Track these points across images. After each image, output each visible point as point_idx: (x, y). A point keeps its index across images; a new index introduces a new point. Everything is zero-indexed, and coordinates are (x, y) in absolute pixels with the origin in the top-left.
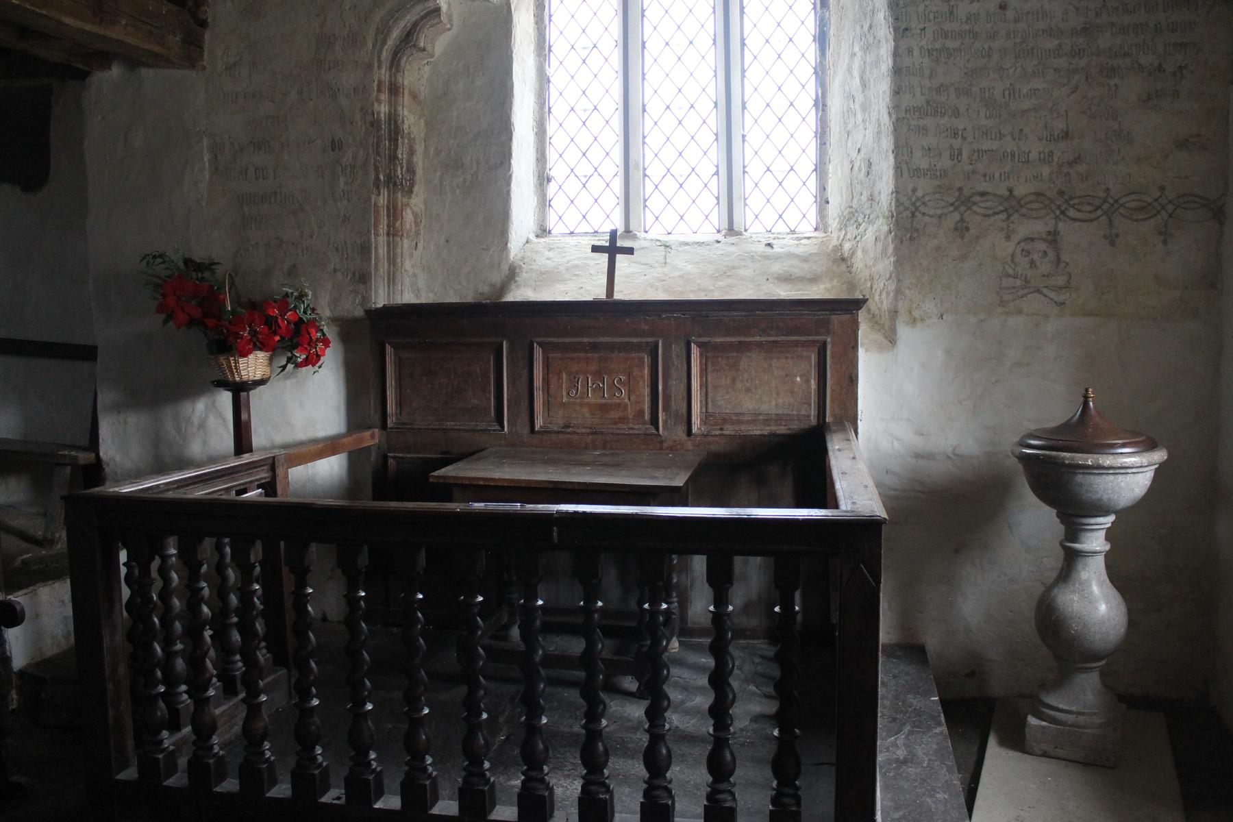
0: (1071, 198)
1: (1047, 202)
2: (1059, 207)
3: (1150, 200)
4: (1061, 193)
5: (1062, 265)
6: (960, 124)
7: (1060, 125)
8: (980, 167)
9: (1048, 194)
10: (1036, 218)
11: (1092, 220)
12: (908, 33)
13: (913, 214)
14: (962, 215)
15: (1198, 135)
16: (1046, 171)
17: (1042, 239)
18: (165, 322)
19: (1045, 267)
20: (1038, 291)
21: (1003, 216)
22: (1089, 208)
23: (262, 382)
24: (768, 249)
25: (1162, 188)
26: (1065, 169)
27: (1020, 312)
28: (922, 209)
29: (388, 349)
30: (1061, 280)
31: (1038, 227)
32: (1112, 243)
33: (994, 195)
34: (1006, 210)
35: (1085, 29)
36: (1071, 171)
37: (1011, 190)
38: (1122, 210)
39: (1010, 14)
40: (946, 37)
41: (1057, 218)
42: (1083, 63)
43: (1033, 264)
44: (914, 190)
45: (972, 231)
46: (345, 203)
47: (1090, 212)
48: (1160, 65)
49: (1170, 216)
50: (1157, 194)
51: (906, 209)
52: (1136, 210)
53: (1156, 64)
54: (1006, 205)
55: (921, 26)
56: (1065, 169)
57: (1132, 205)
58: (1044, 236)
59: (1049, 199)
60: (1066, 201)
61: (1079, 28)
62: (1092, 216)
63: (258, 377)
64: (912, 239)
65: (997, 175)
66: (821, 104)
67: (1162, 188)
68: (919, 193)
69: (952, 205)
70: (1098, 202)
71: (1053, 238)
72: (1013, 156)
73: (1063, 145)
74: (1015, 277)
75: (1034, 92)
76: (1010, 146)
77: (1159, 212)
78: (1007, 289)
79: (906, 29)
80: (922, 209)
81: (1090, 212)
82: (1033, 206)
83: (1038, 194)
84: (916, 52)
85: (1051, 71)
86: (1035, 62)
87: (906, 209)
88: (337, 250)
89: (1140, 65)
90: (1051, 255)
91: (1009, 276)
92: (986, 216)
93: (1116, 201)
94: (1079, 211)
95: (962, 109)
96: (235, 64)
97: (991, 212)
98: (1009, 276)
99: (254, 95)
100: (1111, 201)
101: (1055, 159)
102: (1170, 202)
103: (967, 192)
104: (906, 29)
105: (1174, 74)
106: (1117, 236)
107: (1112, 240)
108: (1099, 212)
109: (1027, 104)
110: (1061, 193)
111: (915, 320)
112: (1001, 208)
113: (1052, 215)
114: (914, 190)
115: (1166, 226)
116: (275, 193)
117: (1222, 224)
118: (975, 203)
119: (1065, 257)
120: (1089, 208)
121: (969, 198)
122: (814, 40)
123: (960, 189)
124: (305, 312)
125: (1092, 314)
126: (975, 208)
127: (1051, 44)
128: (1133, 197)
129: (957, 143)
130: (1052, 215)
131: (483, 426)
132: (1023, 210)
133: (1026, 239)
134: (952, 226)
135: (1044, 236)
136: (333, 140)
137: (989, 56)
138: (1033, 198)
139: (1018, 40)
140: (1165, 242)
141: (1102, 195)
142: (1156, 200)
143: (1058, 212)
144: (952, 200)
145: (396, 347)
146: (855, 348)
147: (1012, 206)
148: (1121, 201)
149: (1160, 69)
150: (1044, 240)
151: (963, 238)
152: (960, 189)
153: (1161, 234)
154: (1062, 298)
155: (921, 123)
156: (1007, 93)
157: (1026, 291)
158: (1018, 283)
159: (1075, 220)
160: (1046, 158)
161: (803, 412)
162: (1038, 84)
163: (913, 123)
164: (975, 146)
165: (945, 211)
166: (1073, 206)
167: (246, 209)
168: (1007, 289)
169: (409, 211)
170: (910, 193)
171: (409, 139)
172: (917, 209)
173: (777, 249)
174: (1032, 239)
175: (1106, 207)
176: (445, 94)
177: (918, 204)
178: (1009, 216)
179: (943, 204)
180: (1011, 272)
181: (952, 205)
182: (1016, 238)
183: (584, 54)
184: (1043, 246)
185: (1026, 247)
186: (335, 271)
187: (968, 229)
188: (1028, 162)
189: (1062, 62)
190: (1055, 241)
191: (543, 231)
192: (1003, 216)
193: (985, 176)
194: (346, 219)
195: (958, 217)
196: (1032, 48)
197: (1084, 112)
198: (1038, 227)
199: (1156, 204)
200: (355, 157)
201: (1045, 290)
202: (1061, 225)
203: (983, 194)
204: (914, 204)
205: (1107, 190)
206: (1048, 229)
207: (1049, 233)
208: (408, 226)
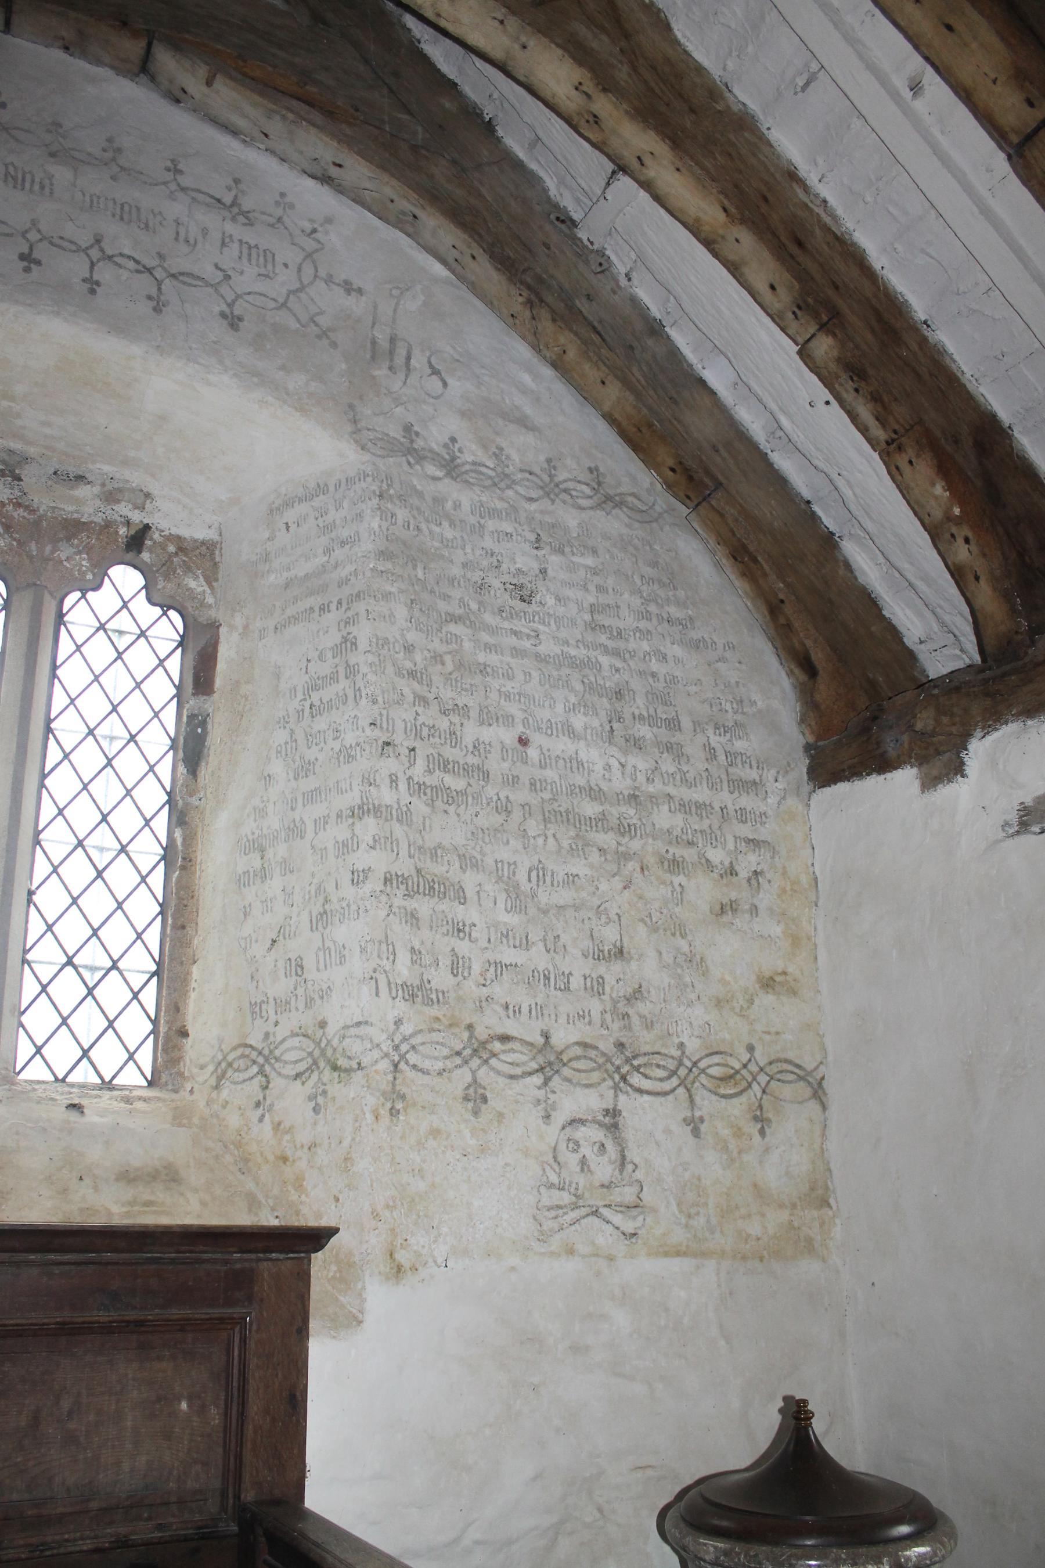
0: (635, 1057)
1: (601, 1060)
2: (618, 1068)
3: (737, 1066)
4: (620, 1046)
5: (630, 1167)
6: (468, 914)
7: (610, 935)
8: (498, 991)
9: (602, 1046)
10: (588, 1086)
11: (665, 1094)
12: (390, 748)
13: (396, 1066)
14: (474, 1073)
15: (784, 973)
16: (595, 1006)
17: (595, 1121)
19: (603, 1169)
20: (595, 1213)
21: (537, 1080)
22: (661, 1073)
24: (73, 1116)
25: (751, 1048)
26: (622, 1007)
27: (571, 1251)
28: (412, 1058)
30: (628, 1194)
31: (590, 1101)
32: (696, 1133)
33: (522, 1041)
34: (541, 1069)
35: (634, 797)
36: (631, 1011)
37: (546, 1036)
38: (703, 1079)
39: (532, 752)
40: (445, 769)
41: (616, 1087)
42: (636, 845)
43: (583, 1162)
44: (398, 1023)
45: (495, 1103)
47: (661, 1080)
48: (731, 863)
49: (764, 1092)
50: (745, 1057)
51: (387, 1055)
52: (721, 1079)
53: (727, 863)
54: (541, 1060)
55: (411, 744)
56: (622, 1007)
57: (715, 1071)
58: (601, 1118)
59: (604, 1054)
60: (628, 1061)
61: (626, 793)
62: (667, 1086)
64: (393, 1112)
65: (525, 1009)
66: (178, 859)
67: (751, 1048)
68: (407, 1029)
69: (458, 1053)
70: (671, 1065)
71: (612, 1121)
72: (547, 978)
73: (617, 967)
74: (561, 1189)
75: (571, 879)
76: (538, 958)
77: (750, 1085)
78: (550, 1209)
79: (388, 744)
80: (412, 1058)
81: (661, 1080)
82: (581, 1065)
83: (585, 1045)
84: (403, 786)
85: (595, 849)
86: (572, 833)
87: (387, 1055)
89: (707, 860)
91: (552, 1186)
92: (512, 1077)
93: (695, 1064)
94: (646, 1076)
95: (470, 892)
97: (518, 1071)
98: (552, 1186)
100: (689, 1064)
101: (607, 988)
102: (762, 1069)
103: (481, 1033)
104: (388, 744)
105: (749, 880)
106: (702, 1120)
107: (694, 1125)
108: (675, 1081)
109: (564, 896)
110: (620, 1046)
111: (399, 1268)
112: (534, 1066)
113: (610, 1083)
114: (398, 1023)
115: (760, 1107)
117: (824, 1108)
118: (494, 1055)
119: (633, 1154)
120: (661, 1073)
121: (484, 1044)
122: (173, 747)
123: (470, 1027)
125: (678, 1253)
126: (493, 1061)
127: (590, 809)
128: (716, 1059)
129: (463, 947)
130: (610, 1083)
132: (566, 1071)
134: (460, 1092)
135: (601, 1118)
137: (509, 813)
138: (578, 1051)
139: (547, 795)
140: (762, 1132)
141: (677, 1053)
142: (745, 1066)
143: (617, 1077)
144: (459, 1047)
146: (302, 1332)
147: (549, 1062)
148: (702, 1064)
149: (732, 872)
150: (601, 1124)
151: (476, 1113)
152: (470, 1027)
153: (756, 1119)
154: (629, 1227)
155: (412, 904)
156: (534, 874)
157: (574, 1215)
158: (566, 1198)
159: (640, 1091)
160: (597, 987)
161: (190, 1484)
162: (578, 867)
163: (398, 902)
164: (489, 955)
165: (448, 1063)
166: (637, 1069)
168: (550, 1209)
170: (392, 1027)
172: (402, 1057)
173: (91, 1117)
174: (582, 1122)
175: (683, 1072)
177: (404, 1047)
178: (547, 1081)
179: (446, 1052)
180: (554, 1179)
181: (458, 1053)
182: (560, 1118)
184: (597, 1134)
187: (485, 1099)
188: (567, 989)
189: (607, 839)
190: (615, 1126)
192: (537, 1080)
193: (507, 1008)
195: (468, 1078)
196: (567, 812)
197: (642, 920)
198: (590, 1101)
199: (744, 1072)
201: (605, 1212)
202: (622, 1098)
203: (505, 1038)
204: (396, 1048)
205: (681, 1045)
206: (605, 1106)
207: (607, 1112)
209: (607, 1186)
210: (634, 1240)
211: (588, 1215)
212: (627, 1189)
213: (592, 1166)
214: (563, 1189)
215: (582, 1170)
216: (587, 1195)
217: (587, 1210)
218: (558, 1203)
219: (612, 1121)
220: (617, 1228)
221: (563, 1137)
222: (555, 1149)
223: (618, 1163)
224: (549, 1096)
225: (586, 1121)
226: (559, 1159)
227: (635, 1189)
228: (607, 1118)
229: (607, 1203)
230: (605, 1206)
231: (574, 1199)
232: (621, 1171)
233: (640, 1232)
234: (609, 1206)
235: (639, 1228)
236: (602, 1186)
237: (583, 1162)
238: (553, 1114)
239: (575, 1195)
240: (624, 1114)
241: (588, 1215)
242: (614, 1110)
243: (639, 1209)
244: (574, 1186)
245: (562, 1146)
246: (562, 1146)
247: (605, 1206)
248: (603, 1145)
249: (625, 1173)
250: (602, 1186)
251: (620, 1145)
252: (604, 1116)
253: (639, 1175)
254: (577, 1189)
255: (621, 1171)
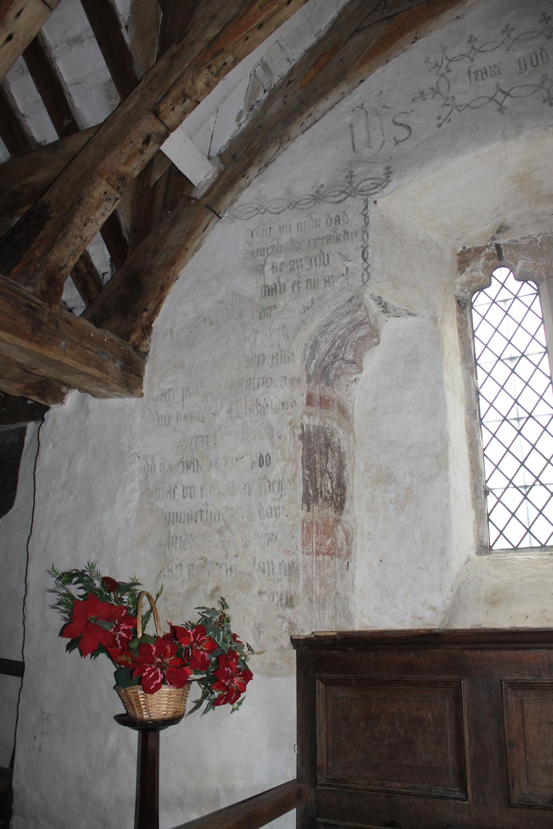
18: (70, 647)
23: (174, 720)
29: (320, 686)
46: (273, 519)
63: (170, 715)
88: (264, 571)
96: (169, 390)
99: (186, 418)
116: (201, 511)
124: (225, 641)
131: (440, 791)
136: (261, 456)
145: (329, 683)
167: (172, 528)
169: (340, 527)
171: (339, 452)
176: (374, 409)
183: (512, 365)
186: (260, 593)
191: (485, 548)
194: (272, 538)
200: (284, 473)
208: (339, 545)
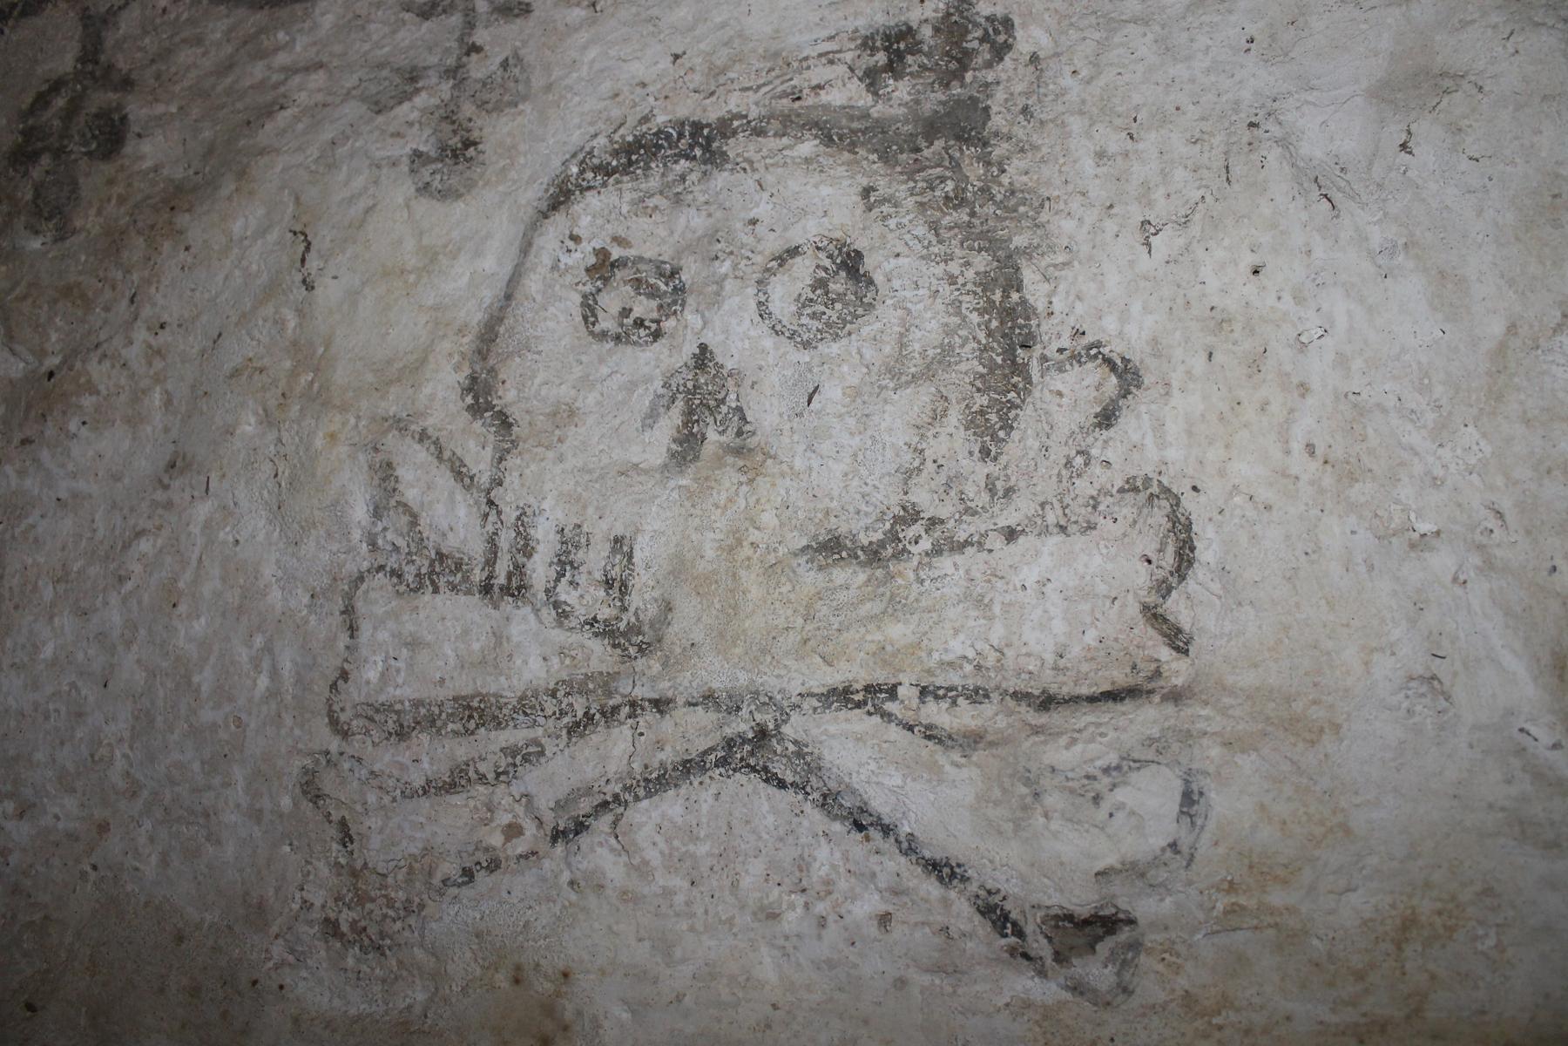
5: (1065, 395)
17: (791, 123)
20: (753, 751)
58: (845, 93)
90: (920, 289)
91: (441, 570)
98: (441, 570)
133: (636, 153)
135: (844, 93)
150: (838, 134)
174: (704, 142)
180: (455, 521)
184: (818, 198)
185: (652, 238)
190: (963, 125)
207: (893, 49)
209: (869, 554)
210: (1097, 971)
211: (689, 767)
212: (1038, 560)
213: (768, 411)
214: (516, 589)
215: (688, 445)
216: (690, 620)
217: (695, 729)
218: (463, 684)
219: (934, 100)
220: (944, 871)
221: (561, 254)
222: (488, 336)
223: (969, 364)
224: (481, 36)
225: (725, 128)
226: (507, 396)
227: (1117, 562)
228: (901, 90)
229: (856, 672)
230: (841, 696)
231: (599, 655)
232: (991, 428)
233: (1146, 908)
234: (872, 697)
235: (1134, 871)
236: (831, 548)
237: (703, 406)
238: (495, 131)
239: (608, 632)
240: (1030, 38)
241: (689, 767)
242: (953, 27)
243: (1145, 719)
244: (595, 559)
245: (551, 318)
246: (551, 318)
247: (841, 696)
248: (851, 263)
249: (1022, 444)
250: (831, 548)
251: (990, 242)
252: (871, 78)
253: (1152, 439)
254: (617, 586)
255: (991, 428)
